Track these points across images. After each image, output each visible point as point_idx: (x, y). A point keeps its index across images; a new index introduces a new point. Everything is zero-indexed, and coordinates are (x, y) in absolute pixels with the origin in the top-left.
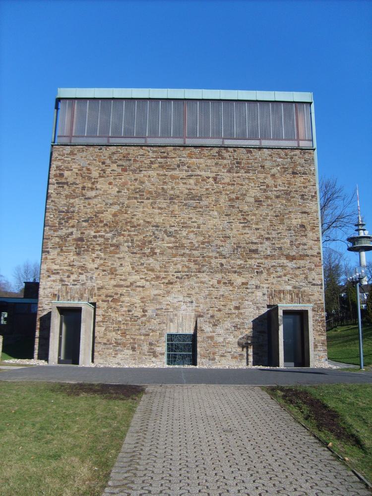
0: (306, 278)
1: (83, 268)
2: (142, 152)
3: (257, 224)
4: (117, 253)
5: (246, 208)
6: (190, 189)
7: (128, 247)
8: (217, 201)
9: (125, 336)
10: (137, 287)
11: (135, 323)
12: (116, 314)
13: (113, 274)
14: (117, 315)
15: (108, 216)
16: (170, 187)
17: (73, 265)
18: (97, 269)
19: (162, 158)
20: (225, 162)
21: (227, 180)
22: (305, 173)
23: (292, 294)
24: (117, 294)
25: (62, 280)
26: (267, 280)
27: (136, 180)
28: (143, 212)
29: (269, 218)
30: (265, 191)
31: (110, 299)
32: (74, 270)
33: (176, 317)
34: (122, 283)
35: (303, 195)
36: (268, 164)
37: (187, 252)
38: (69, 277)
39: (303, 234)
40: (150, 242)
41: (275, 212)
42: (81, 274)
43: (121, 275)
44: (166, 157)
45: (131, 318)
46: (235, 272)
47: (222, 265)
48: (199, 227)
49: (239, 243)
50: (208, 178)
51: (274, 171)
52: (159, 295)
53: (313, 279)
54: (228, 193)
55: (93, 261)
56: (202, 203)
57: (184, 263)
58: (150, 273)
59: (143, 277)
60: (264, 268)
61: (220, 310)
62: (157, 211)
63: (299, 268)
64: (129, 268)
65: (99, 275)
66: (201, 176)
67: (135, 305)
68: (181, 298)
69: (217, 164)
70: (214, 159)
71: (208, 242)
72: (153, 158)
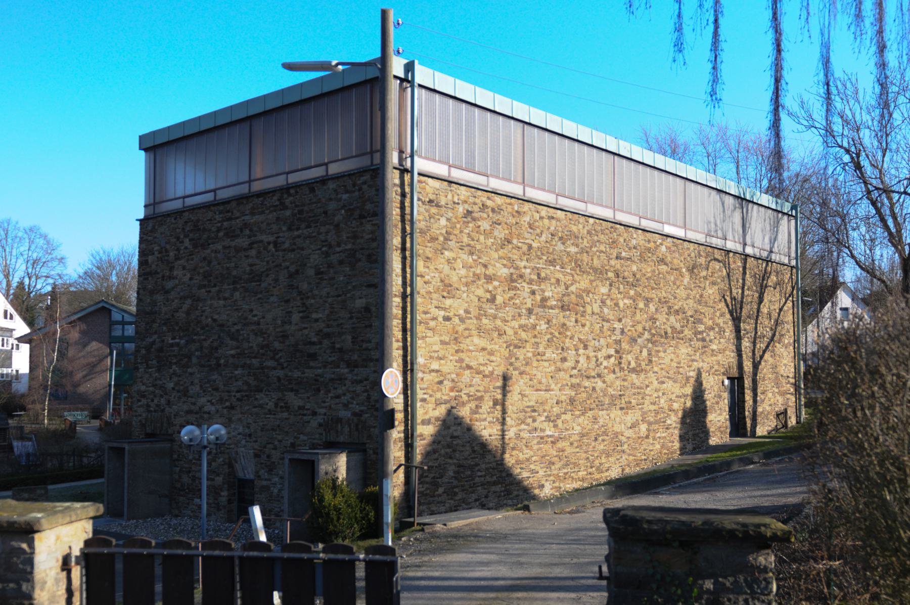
0: (368, 398)
1: (162, 387)
2: (210, 215)
3: (316, 312)
5: (304, 286)
6: (251, 265)
7: (198, 357)
8: (276, 280)
13: (185, 395)
15: (181, 315)
16: (233, 265)
18: (173, 389)
20: (288, 213)
21: (287, 245)
23: (350, 425)
25: (148, 406)
26: (324, 402)
27: (205, 259)
28: (211, 306)
29: (330, 300)
30: (327, 254)
34: (193, 407)
35: (369, 256)
36: (332, 206)
37: (248, 362)
38: (153, 401)
41: (337, 289)
42: (162, 396)
44: (230, 219)
46: (292, 390)
47: (279, 379)
48: (259, 324)
50: (269, 243)
51: (338, 218)
54: (288, 264)
55: (171, 378)
56: (264, 285)
57: (245, 378)
58: (215, 393)
59: (210, 398)
61: (275, 448)
62: (222, 302)
63: (361, 381)
66: (261, 241)
68: (241, 429)
69: (278, 219)
70: (275, 211)
72: (219, 222)
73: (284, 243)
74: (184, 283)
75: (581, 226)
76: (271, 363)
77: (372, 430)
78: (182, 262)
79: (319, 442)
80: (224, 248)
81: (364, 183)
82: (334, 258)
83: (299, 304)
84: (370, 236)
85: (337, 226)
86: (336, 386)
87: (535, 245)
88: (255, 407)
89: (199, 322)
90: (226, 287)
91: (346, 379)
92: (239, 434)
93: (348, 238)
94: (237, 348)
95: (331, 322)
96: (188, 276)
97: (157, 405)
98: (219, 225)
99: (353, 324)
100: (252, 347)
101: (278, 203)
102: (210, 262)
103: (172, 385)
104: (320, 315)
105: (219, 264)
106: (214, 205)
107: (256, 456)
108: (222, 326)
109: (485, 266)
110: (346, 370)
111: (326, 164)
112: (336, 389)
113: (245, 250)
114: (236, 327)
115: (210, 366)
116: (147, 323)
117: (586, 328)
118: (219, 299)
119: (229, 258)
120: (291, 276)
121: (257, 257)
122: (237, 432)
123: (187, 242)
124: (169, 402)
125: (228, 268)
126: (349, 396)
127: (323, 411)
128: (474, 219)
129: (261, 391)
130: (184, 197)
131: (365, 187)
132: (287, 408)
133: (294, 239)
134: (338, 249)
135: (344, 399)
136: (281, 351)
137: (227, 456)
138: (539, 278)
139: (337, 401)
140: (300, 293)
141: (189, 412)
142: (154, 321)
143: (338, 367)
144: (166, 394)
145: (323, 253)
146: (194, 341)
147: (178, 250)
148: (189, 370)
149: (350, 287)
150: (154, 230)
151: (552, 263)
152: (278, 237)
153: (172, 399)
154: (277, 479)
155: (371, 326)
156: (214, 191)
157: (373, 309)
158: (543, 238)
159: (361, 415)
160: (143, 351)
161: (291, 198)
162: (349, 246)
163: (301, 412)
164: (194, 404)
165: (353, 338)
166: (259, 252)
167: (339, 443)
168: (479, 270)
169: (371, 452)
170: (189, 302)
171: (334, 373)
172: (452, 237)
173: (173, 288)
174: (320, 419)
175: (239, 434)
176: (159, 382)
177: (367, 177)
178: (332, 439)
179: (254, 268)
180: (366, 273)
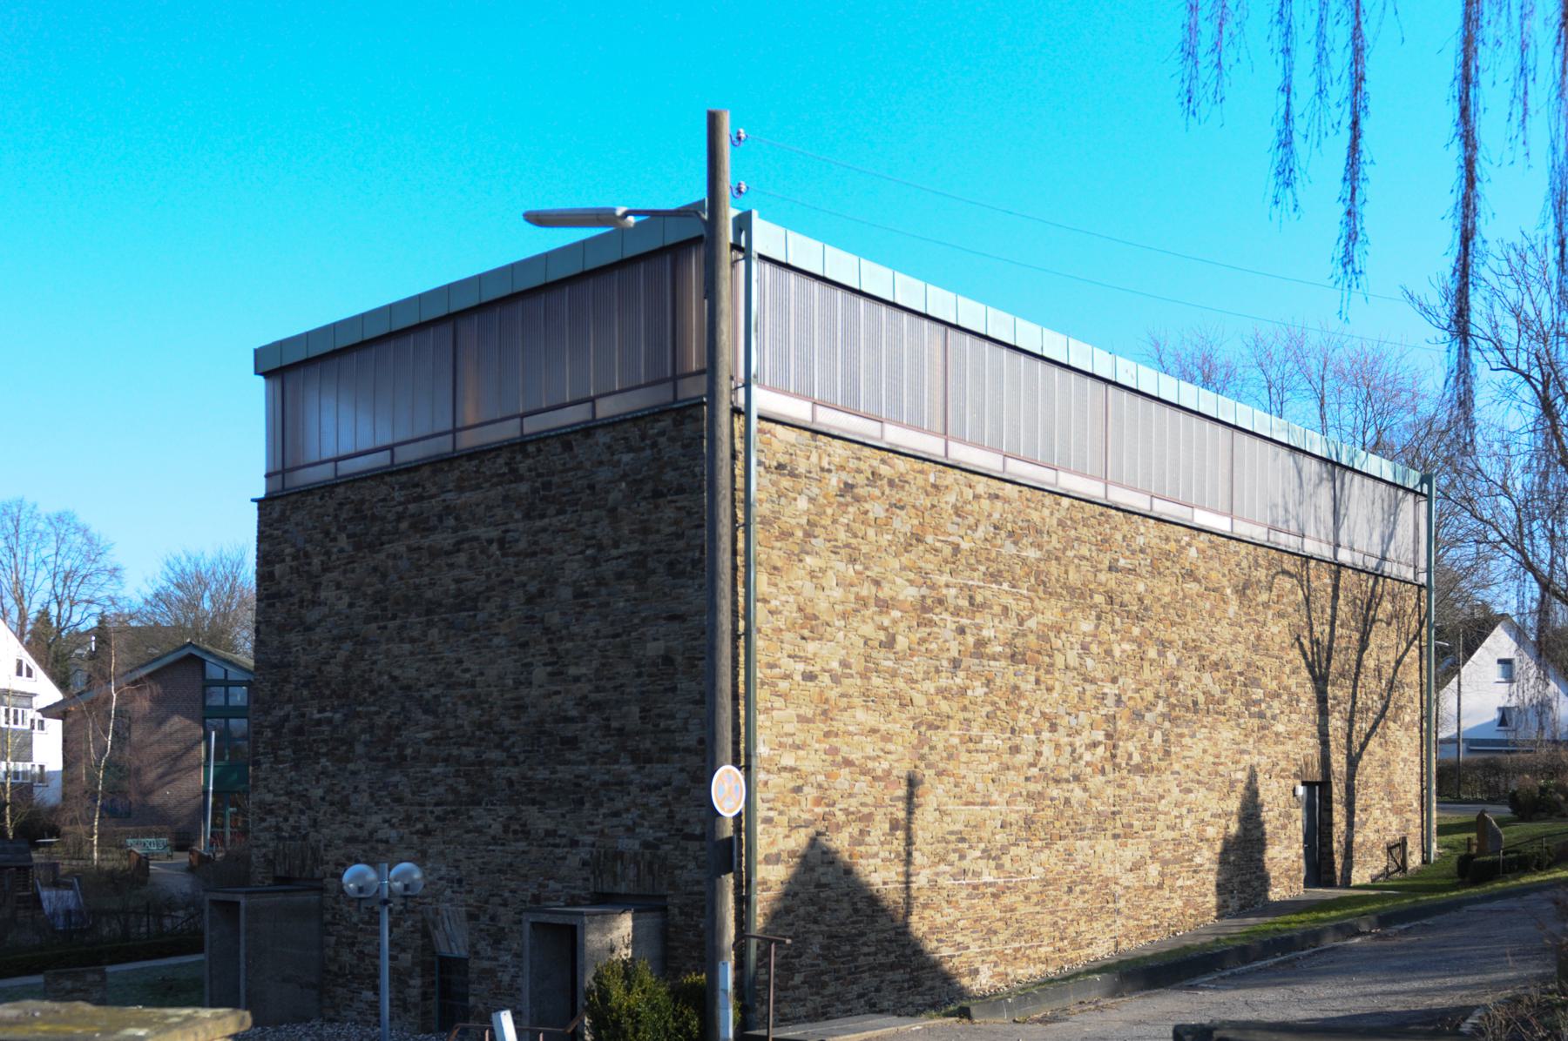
0: (671, 816)
1: (302, 796)
3: (577, 664)
4: (349, 761)
5: (555, 619)
6: (458, 581)
7: (366, 744)
10: (378, 841)
13: (343, 811)
15: (334, 669)
16: (425, 580)
17: (292, 793)
18: (323, 799)
19: (415, 500)
20: (524, 488)
21: (522, 545)
22: (680, 490)
23: (637, 864)
25: (278, 829)
26: (592, 823)
27: (375, 569)
29: (600, 643)
30: (595, 562)
34: (358, 832)
35: (671, 564)
37: (455, 752)
38: (286, 820)
39: (667, 684)
40: (398, 728)
41: (613, 623)
42: (302, 812)
44: (420, 498)
46: (533, 802)
47: (511, 783)
48: (473, 685)
49: (542, 722)
50: (490, 542)
51: (614, 496)
53: (686, 822)
54: (524, 578)
56: (481, 616)
57: (449, 781)
58: (397, 807)
59: (388, 816)
60: (588, 789)
61: (505, 905)
62: (407, 647)
63: (657, 787)
64: (365, 798)
66: (476, 539)
69: (506, 498)
70: (500, 483)
71: (489, 723)
72: (400, 504)
73: (517, 541)
74: (338, 613)
75: (1046, 512)
76: (495, 755)
77: (677, 872)
78: (335, 575)
79: (583, 893)
80: (410, 549)
81: (662, 433)
82: (607, 569)
83: (545, 648)
84: (673, 529)
85: (613, 511)
86: (612, 794)
87: (965, 545)
88: (468, 832)
89: (368, 681)
90: (413, 619)
91: (631, 783)
92: (441, 879)
93: (632, 532)
94: (435, 727)
95: (603, 683)
96: (346, 599)
97: (294, 828)
98: (400, 509)
99: (643, 685)
100: (462, 726)
101: (505, 470)
102: (384, 576)
103: (320, 792)
104: (584, 670)
105: (401, 578)
106: (391, 474)
107: (472, 917)
108: (409, 688)
109: (877, 583)
110: (631, 768)
111: (592, 400)
112: (612, 800)
113: (448, 553)
114: (433, 691)
115: (388, 759)
116: (275, 684)
117: (1055, 694)
118: (402, 641)
119: (419, 569)
120: (530, 600)
121: (470, 567)
122: (436, 875)
123: (343, 540)
124: (315, 823)
125: (417, 587)
126: (635, 812)
127: (589, 839)
128: (857, 499)
129: (479, 804)
130: (337, 460)
131: (662, 440)
132: (525, 833)
133: (536, 533)
134: (614, 553)
135: (627, 819)
136: (513, 732)
137: (419, 917)
138: (972, 604)
139: (615, 821)
140: (547, 630)
141: (351, 840)
142: (286, 680)
143: (616, 762)
144: (310, 808)
145: (587, 559)
146: (358, 715)
147: (328, 553)
148: (351, 766)
149: (636, 621)
150: (283, 518)
151: (995, 577)
152: (507, 531)
154: (508, 958)
155: (674, 689)
156: (391, 448)
157: (679, 659)
158: (980, 533)
159: (657, 847)
160: (268, 733)
161: (530, 461)
162: (634, 547)
163: (551, 840)
164: (361, 826)
165: (643, 710)
166: (472, 558)
167: (618, 895)
168: (866, 590)
169: (676, 911)
170: (348, 646)
171: (609, 772)
172: (818, 531)
173: (319, 621)
174: (584, 853)
175: (441, 879)
176: (295, 787)
177: (666, 422)
178: (606, 889)
179: (462, 586)
180: (665, 594)
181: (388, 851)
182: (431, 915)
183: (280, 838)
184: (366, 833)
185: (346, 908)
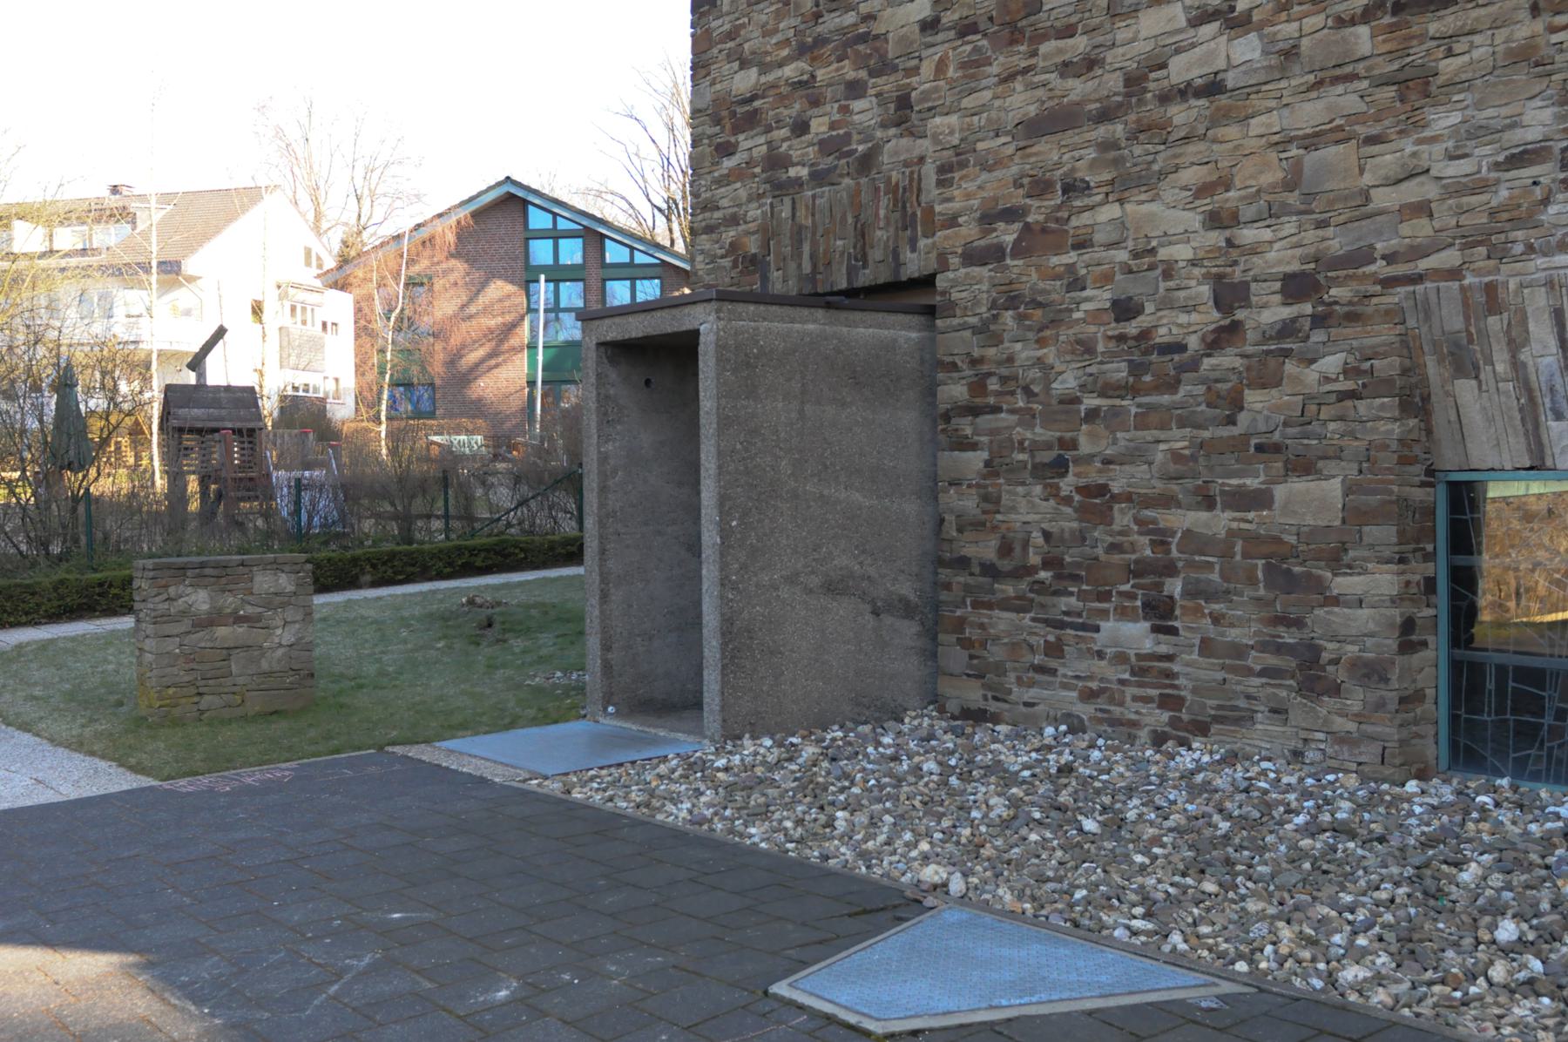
9: (1105, 517)
11: (1166, 399)
12: (1042, 343)
14: (1049, 354)
17: (820, 41)
18: (930, 26)
24: (1041, 187)
25: (776, 161)
31: (1007, 235)
32: (821, 74)
33: (1494, 322)
38: (801, 128)
42: (855, 89)
43: (1068, 32)
45: (1136, 369)
52: (1338, 135)
65: (941, 67)
67: (1163, 254)
92: (1518, 160)
122: (1484, 155)
137: (1382, 334)
144: (884, 67)
153: (923, 82)
164: (1090, 64)
175: (1518, 160)
181: (1220, 118)
182: (1452, 319)
183: (781, 188)
184: (1114, 82)
185: (1024, 353)
